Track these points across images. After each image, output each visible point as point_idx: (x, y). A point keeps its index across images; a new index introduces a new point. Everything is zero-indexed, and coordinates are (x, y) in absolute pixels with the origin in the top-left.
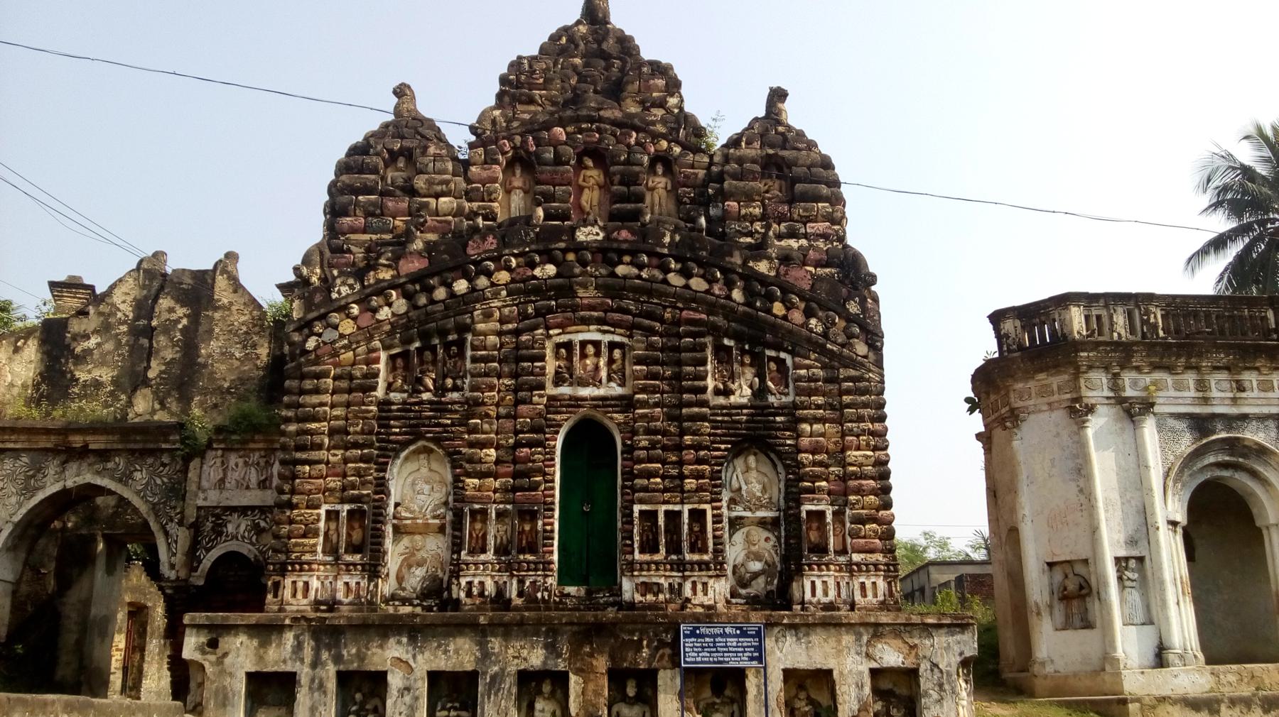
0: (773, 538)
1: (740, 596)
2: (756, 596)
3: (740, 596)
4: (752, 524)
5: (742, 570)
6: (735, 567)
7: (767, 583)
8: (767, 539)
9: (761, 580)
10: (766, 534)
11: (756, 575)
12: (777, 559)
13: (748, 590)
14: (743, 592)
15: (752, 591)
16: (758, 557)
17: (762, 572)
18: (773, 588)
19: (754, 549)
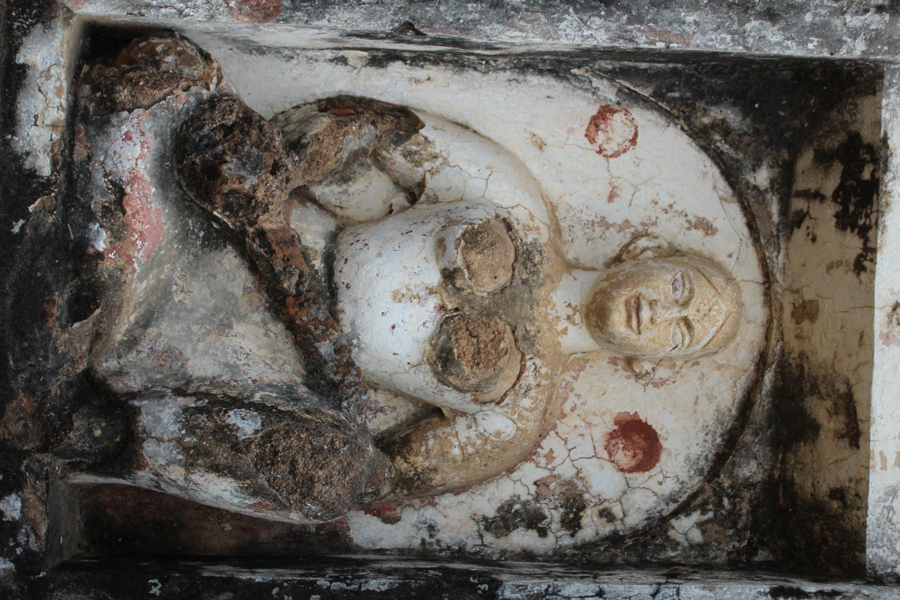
0: (639, 498)
1: (90, 115)
2: (91, 296)
3: (90, 115)
4: (789, 307)
5: (369, 190)
6: (404, 121)
7: (212, 403)
8: (638, 440)
9: (253, 353)
10: (689, 415)
11: (302, 301)
12: (455, 520)
13: (152, 214)
14: (133, 150)
15: (146, 242)
16: (470, 339)
17: (330, 373)
18: (162, 463)
19: (560, 301)
